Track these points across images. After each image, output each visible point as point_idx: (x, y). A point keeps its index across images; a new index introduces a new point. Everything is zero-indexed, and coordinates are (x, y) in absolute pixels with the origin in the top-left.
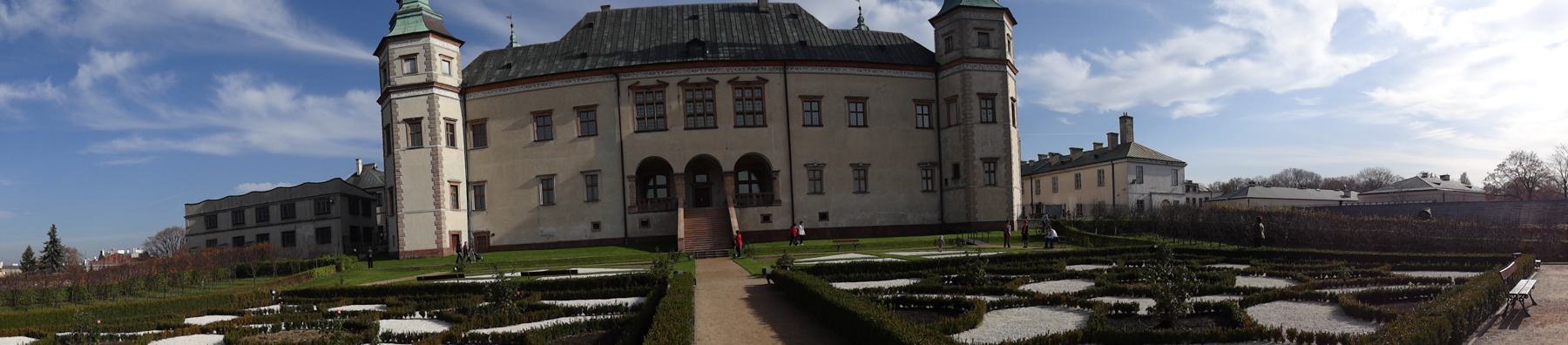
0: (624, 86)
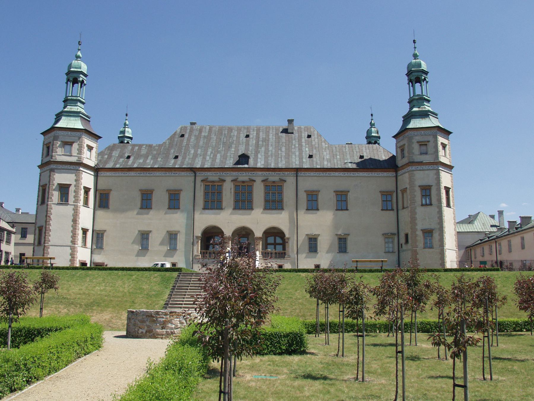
0: (199, 179)
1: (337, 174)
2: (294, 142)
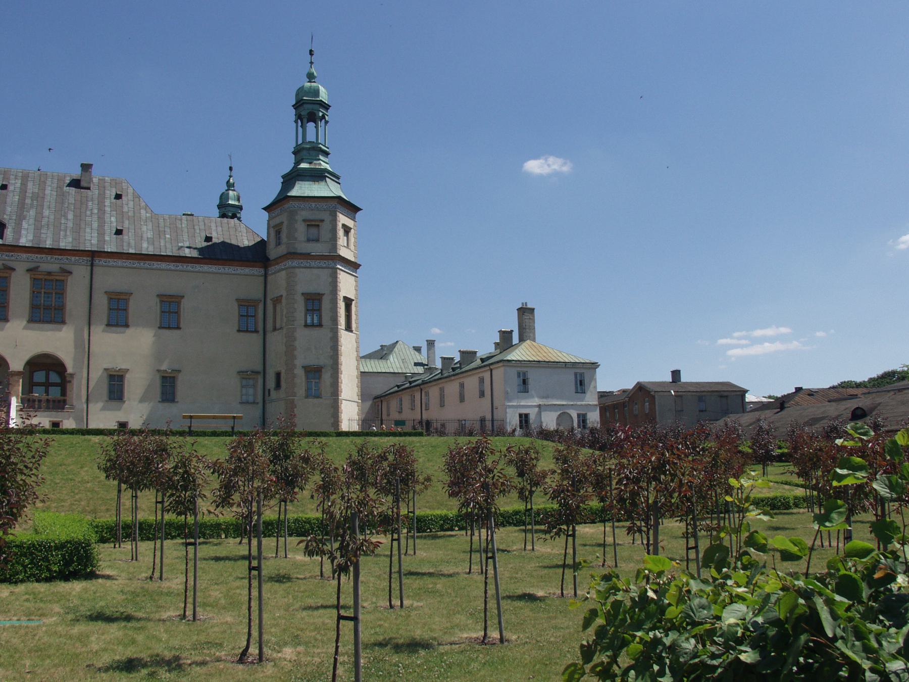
1: (164, 265)
2: (90, 204)
